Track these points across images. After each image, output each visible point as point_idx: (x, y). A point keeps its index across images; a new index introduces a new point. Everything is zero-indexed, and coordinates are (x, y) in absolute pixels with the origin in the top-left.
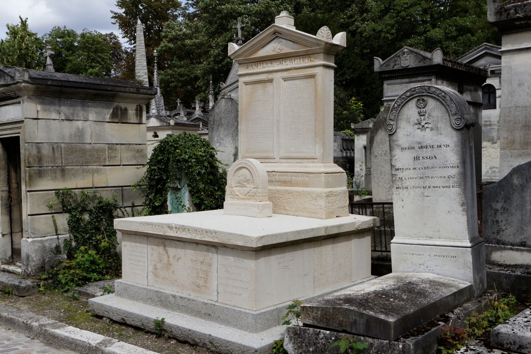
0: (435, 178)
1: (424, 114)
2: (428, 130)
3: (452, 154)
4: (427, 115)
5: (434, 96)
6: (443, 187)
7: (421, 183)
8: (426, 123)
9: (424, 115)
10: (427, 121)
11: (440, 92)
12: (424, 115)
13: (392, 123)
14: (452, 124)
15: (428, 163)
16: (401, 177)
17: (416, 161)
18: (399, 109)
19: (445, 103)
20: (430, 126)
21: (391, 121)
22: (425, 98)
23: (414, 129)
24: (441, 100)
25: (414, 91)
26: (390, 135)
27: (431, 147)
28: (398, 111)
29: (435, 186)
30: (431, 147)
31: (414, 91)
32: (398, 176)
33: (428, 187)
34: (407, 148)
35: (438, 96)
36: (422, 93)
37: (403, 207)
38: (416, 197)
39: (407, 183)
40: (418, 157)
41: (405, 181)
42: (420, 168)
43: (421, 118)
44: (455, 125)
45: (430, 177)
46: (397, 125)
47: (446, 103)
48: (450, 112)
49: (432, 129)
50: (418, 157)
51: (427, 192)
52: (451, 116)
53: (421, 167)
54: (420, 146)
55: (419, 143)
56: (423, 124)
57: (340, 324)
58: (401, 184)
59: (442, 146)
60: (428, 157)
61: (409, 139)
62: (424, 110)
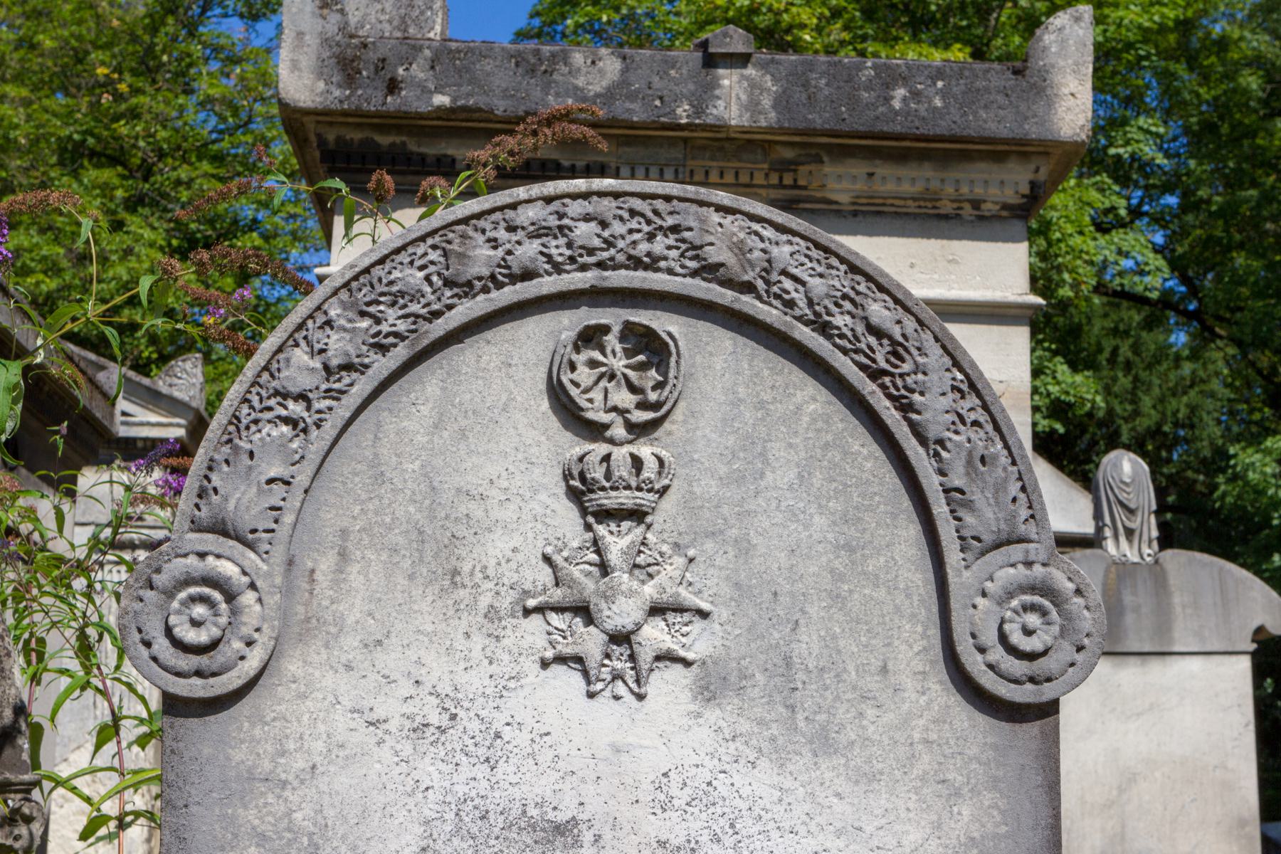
1: (645, 499)
4: (666, 512)
5: (771, 314)
8: (656, 610)
9: (637, 515)
11: (841, 281)
12: (637, 515)
13: (228, 569)
14: (965, 648)
19: (891, 416)
21: (210, 541)
23: (505, 666)
24: (845, 366)
25: (539, 232)
28: (319, 440)
31: (539, 232)
35: (824, 328)
36: (636, 263)
44: (997, 654)
46: (288, 591)
47: (906, 408)
48: (940, 509)
52: (953, 556)
61: (429, 770)
62: (645, 451)
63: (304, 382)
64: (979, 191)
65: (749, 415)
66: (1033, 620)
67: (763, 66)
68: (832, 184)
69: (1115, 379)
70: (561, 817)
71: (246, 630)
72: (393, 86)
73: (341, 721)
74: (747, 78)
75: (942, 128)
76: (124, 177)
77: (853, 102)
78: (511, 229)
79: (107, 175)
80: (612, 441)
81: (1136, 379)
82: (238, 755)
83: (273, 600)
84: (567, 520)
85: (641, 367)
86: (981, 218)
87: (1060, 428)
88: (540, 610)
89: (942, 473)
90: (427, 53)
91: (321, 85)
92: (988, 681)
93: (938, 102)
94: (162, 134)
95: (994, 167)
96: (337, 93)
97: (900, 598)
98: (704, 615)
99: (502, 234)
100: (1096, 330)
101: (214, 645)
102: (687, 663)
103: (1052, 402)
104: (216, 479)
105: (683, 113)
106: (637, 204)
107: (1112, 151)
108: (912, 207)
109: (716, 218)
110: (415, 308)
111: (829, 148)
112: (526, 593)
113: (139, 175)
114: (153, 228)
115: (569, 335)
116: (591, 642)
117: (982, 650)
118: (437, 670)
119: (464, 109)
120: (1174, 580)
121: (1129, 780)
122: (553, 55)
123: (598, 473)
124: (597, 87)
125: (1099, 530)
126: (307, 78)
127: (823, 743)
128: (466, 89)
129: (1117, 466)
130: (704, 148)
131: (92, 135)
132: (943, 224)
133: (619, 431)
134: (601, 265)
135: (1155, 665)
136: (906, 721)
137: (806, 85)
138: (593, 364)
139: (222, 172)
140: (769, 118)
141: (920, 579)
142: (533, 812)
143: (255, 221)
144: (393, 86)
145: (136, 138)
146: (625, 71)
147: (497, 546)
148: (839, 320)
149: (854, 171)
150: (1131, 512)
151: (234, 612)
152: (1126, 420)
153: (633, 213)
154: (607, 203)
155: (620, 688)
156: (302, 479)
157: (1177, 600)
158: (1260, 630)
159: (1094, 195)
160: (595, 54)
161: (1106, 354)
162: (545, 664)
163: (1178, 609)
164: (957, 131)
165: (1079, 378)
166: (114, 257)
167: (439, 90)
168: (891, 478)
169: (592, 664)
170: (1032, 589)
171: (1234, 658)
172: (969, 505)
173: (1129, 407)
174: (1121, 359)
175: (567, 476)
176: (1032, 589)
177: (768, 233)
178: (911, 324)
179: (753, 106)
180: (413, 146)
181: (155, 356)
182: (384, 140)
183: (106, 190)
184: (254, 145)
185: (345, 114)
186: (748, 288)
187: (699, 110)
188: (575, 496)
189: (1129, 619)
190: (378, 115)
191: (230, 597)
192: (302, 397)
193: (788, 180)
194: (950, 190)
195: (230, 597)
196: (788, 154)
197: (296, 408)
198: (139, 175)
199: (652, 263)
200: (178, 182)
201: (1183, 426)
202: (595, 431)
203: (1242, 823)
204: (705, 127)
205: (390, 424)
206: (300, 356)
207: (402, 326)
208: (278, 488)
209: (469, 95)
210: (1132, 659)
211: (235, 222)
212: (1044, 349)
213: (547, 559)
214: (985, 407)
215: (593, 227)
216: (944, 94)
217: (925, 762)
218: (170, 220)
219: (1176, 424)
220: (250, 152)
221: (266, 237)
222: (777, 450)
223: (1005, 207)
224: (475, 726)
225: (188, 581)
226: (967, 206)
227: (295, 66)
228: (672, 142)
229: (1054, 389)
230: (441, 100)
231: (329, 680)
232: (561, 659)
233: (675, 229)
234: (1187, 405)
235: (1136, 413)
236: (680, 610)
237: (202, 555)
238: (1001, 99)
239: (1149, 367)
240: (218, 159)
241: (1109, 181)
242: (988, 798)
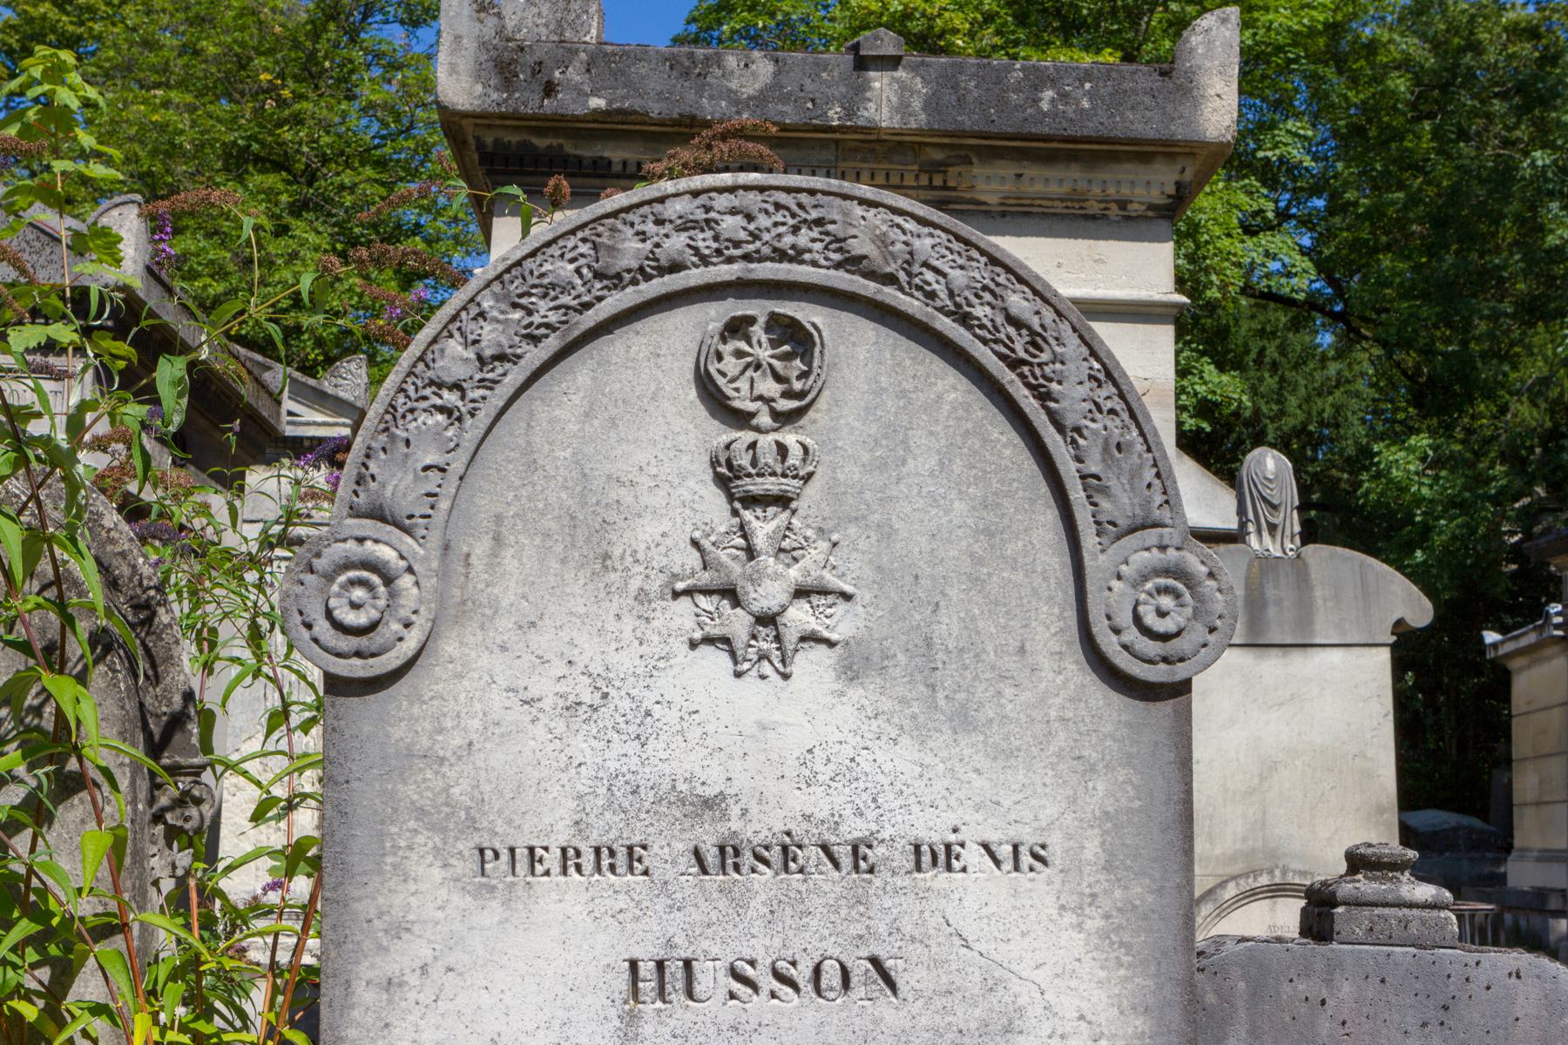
1: (790, 485)
2: (812, 665)
3: (1073, 942)
4: (811, 498)
5: (912, 305)
8: (801, 593)
9: (783, 501)
11: (981, 272)
12: (783, 501)
13: (386, 553)
14: (1100, 629)
17: (651, 1007)
18: (497, 398)
19: (1029, 404)
20: (842, 623)
21: (368, 527)
23: (655, 648)
24: (986, 356)
25: (686, 225)
28: (474, 428)
31: (686, 225)
34: (552, 860)
35: (964, 319)
36: (781, 255)
40: (675, 969)
43: (744, 531)
44: (1132, 635)
47: (1044, 397)
48: (1077, 494)
50: (675, 969)
52: (1089, 540)
55: (708, 803)
59: (973, 856)
60: (802, 974)
61: (581, 746)
62: (790, 438)
63: (458, 372)
64: (1125, 191)
65: (891, 404)
66: (1166, 602)
67: (914, 68)
68: (981, 185)
69: (1261, 380)
70: (710, 792)
71: (404, 613)
72: (550, 89)
73: (497, 699)
74: (897, 80)
75: (1090, 128)
76: (288, 182)
77: (1002, 102)
78: (659, 222)
79: (272, 180)
80: (757, 429)
81: (1282, 379)
82: (398, 732)
83: (430, 583)
84: (714, 506)
85: (786, 357)
86: (1128, 218)
87: (1207, 427)
88: (688, 592)
89: (1079, 459)
90: (583, 56)
91: (479, 88)
92: (1123, 661)
93: (1086, 104)
94: (325, 140)
95: (1141, 168)
96: (495, 96)
97: (1037, 581)
98: (847, 597)
99: (650, 227)
100: (1243, 331)
101: (372, 627)
102: (831, 644)
103: (1199, 402)
104: (373, 467)
105: (834, 115)
106: (782, 198)
107: (1260, 154)
108: (1059, 207)
109: (859, 211)
110: (566, 299)
111: (978, 150)
112: (675, 577)
113: (303, 180)
114: (319, 233)
115: (716, 326)
116: (738, 623)
117: (1117, 631)
118: (590, 651)
119: (620, 111)
120: (1315, 574)
121: (1270, 768)
122: (707, 58)
123: (744, 460)
124: (750, 90)
125: (1243, 525)
126: (465, 81)
127: (963, 720)
128: (622, 92)
129: (1261, 462)
130: (856, 150)
131: (257, 141)
132: (1090, 224)
133: (765, 420)
134: (747, 258)
135: (1297, 659)
136: (1042, 700)
137: (955, 87)
138: (739, 354)
139: (384, 177)
140: (918, 120)
141: (1056, 562)
142: (682, 787)
143: (417, 225)
144: (550, 89)
145: (300, 144)
146: (776, 74)
147: (647, 531)
148: (980, 311)
149: (1003, 172)
150: (1275, 507)
151: (393, 595)
152: (1272, 420)
153: (778, 206)
154: (753, 198)
155: (766, 668)
156: (457, 466)
157: (1318, 593)
158: (1400, 623)
159: (1242, 198)
160: (747, 57)
161: (1253, 355)
162: (693, 645)
163: (1320, 602)
164: (1105, 132)
165: (1225, 378)
166: (280, 261)
167: (595, 93)
168: (1029, 465)
169: (739, 645)
170: (1166, 572)
171: (1374, 650)
172: (1104, 491)
173: (1275, 407)
174: (1267, 360)
175: (714, 463)
176: (1166, 572)
177: (910, 225)
178: (1049, 315)
179: (903, 108)
180: (569, 149)
181: (321, 358)
182: (541, 143)
183: (271, 195)
184: (415, 151)
185: (503, 116)
186: (890, 280)
187: (850, 112)
188: (722, 482)
189: (1272, 612)
190: (534, 118)
191: (388, 581)
192: (456, 386)
193: (938, 181)
194: (1097, 190)
195: (388, 581)
196: (938, 155)
197: (450, 398)
198: (303, 180)
199: (797, 255)
200: (342, 187)
201: (1328, 426)
202: (741, 419)
203: (1381, 810)
204: (856, 129)
205: (542, 413)
206: (454, 346)
207: (553, 318)
208: (434, 475)
209: (625, 98)
210: (1274, 651)
211: (398, 226)
212: (1192, 350)
213: (695, 544)
214: (1122, 396)
215: (739, 220)
216: (1091, 95)
217: (1062, 739)
218: (334, 225)
219: (1322, 424)
220: (412, 157)
221: (429, 242)
222: (918, 438)
223: (1151, 207)
224: (626, 704)
225: (348, 565)
226: (1114, 207)
227: (453, 69)
228: (824, 144)
229: (1201, 389)
230: (597, 103)
231: (485, 660)
232: (709, 640)
233: (819, 222)
234: (1333, 405)
235: (1282, 413)
236: (824, 592)
237: (361, 540)
238: (1147, 100)
239: (1296, 367)
240: (381, 164)
241: (1258, 184)
242: (1122, 774)
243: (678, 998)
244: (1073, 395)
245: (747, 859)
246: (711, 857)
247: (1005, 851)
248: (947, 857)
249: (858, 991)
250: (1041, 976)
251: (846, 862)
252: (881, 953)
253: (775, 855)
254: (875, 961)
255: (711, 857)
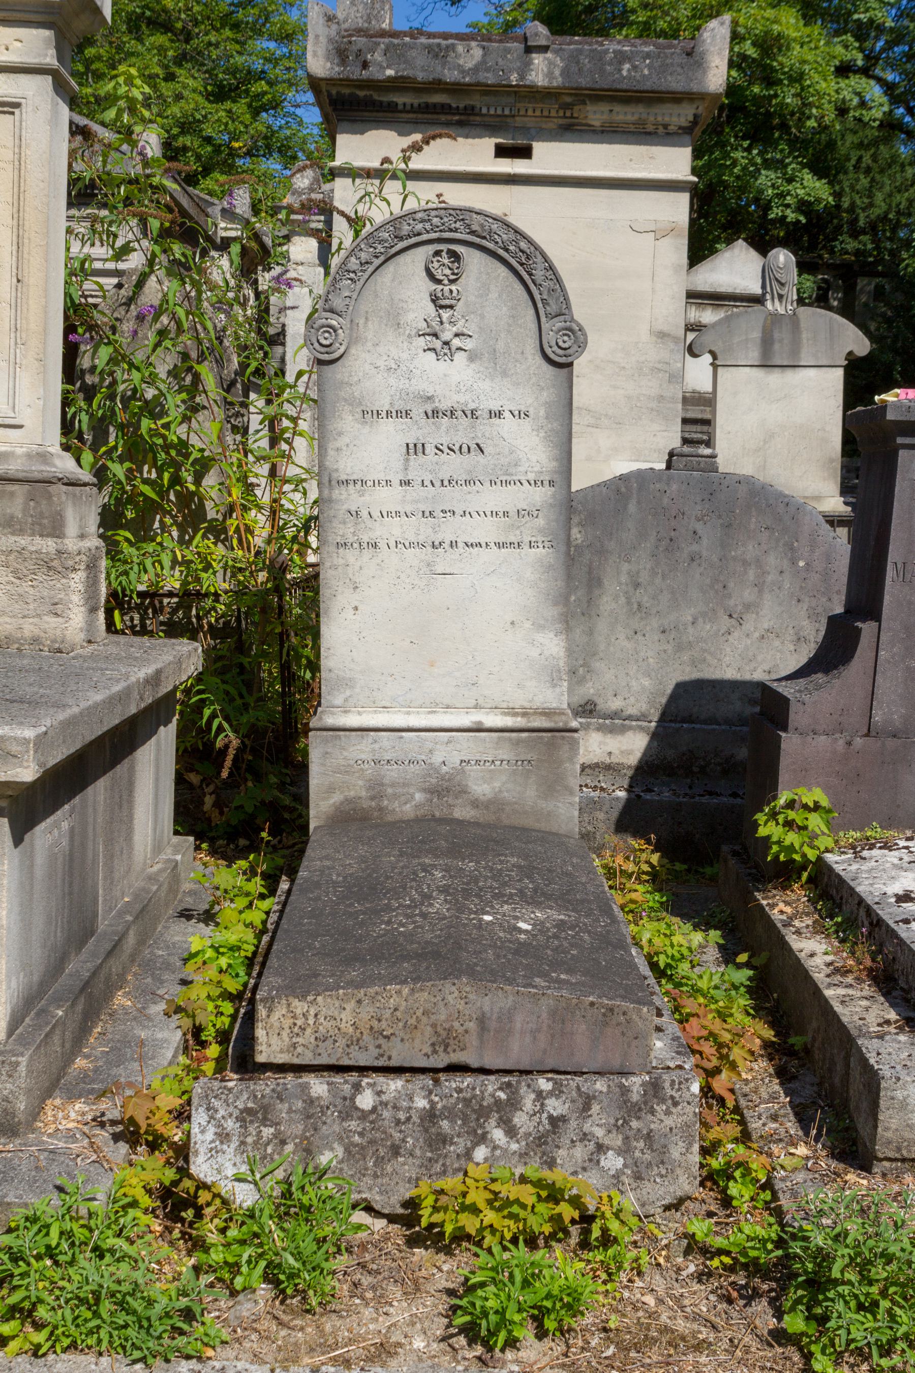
0: (474, 514)
1: (453, 302)
2: (460, 357)
4: (460, 306)
5: (491, 246)
6: (499, 545)
7: (424, 530)
8: (457, 335)
10: (459, 327)
11: (512, 236)
12: (451, 307)
13: (334, 323)
14: (546, 347)
15: (454, 465)
16: (353, 509)
17: (412, 457)
19: (526, 277)
20: (469, 344)
21: (329, 315)
22: (459, 249)
24: (513, 262)
25: (422, 221)
26: (320, 362)
27: (469, 413)
29: (470, 540)
30: (469, 413)
31: (422, 221)
32: (345, 507)
33: (448, 542)
34: (384, 414)
35: (507, 250)
36: (451, 230)
37: (356, 608)
38: (403, 576)
39: (383, 531)
40: (419, 446)
41: (369, 522)
42: (427, 483)
43: (440, 317)
44: (555, 348)
45: (459, 512)
46: (351, 329)
47: (530, 275)
48: (540, 305)
49: (473, 357)
50: (419, 446)
51: (444, 560)
52: (543, 319)
53: (430, 477)
54: (429, 408)
55: (429, 398)
56: (447, 336)
57: (444, 1041)
58: (354, 534)
59: (507, 414)
60: (456, 448)
61: (392, 381)
62: (453, 288)
63: (355, 267)
64: (667, 119)
65: (484, 277)
66: (566, 338)
67: (556, 52)
68: (591, 116)
69: (857, 180)
72: (365, 65)
73: (367, 366)
74: (547, 59)
75: (648, 86)
76: (172, 41)
77: (602, 71)
79: (160, 39)
81: (873, 180)
82: (339, 376)
83: (347, 332)
84: (431, 307)
85: (453, 262)
86: (668, 134)
87: (803, 219)
90: (382, 46)
91: (329, 65)
92: (552, 356)
93: (646, 72)
94: (197, 8)
95: (676, 106)
96: (337, 69)
100: (848, 144)
101: (331, 345)
103: (799, 201)
105: (514, 79)
106: (452, 212)
107: (856, 16)
108: (632, 128)
109: (475, 216)
111: (590, 96)
113: (182, 38)
114: (195, 78)
115: (431, 253)
116: (438, 344)
118: (394, 353)
119: (402, 77)
120: (803, 325)
121: (770, 436)
122: (447, 47)
123: (440, 295)
124: (470, 65)
125: (764, 295)
126: (322, 61)
127: (505, 374)
128: (403, 66)
129: (776, 257)
130: (525, 97)
131: (149, 9)
132: (648, 137)
133: (446, 282)
135: (789, 373)
136: (528, 368)
137: (578, 63)
139: (239, 36)
140: (558, 81)
141: (534, 326)
143: (263, 72)
144: (365, 65)
145: (179, 12)
146: (484, 55)
147: (411, 316)
148: (512, 248)
149: (602, 109)
150: (782, 285)
152: (864, 210)
154: (443, 212)
156: (354, 297)
157: (804, 335)
158: (850, 353)
159: (839, 49)
160: (469, 45)
161: (853, 162)
163: (805, 341)
164: (655, 88)
165: (818, 184)
166: (169, 100)
167: (389, 67)
168: (526, 296)
170: (566, 329)
172: (548, 304)
173: (866, 201)
174: (864, 165)
176: (566, 329)
178: (532, 249)
179: (550, 74)
180: (376, 97)
181: (200, 169)
182: (361, 93)
183: (161, 50)
184: (260, 16)
185: (341, 80)
186: (484, 238)
187: (522, 77)
188: (433, 301)
189: (777, 346)
190: (358, 80)
191: (335, 331)
192: (354, 272)
193: (568, 114)
194: (652, 119)
195: (335, 331)
196: (568, 99)
197: (352, 275)
198: (182, 38)
199: (456, 230)
200: (210, 44)
201: (903, 214)
202: (439, 282)
203: (831, 461)
204: (525, 86)
205: (379, 280)
206: (353, 259)
209: (404, 70)
210: (776, 369)
211: (249, 72)
212: (798, 163)
216: (649, 67)
217: (534, 380)
218: (206, 72)
219: (898, 213)
220: (257, 20)
221: (271, 84)
222: (492, 287)
223: (680, 128)
225: (323, 326)
226: (661, 128)
227: (315, 54)
228: (508, 94)
229: (801, 192)
230: (390, 72)
231: (364, 355)
232: (429, 349)
234: (908, 199)
235: (871, 205)
236: (463, 335)
238: (679, 69)
239: (882, 171)
240: (236, 26)
241: (851, 39)
242: (552, 390)
243: (420, 454)
244: (539, 274)
245: (440, 414)
246: (430, 414)
247: (516, 413)
248: (499, 414)
249: (473, 453)
250: (526, 450)
251: (469, 416)
252: (479, 442)
253: (448, 413)
254: (478, 445)
255: (430, 414)
